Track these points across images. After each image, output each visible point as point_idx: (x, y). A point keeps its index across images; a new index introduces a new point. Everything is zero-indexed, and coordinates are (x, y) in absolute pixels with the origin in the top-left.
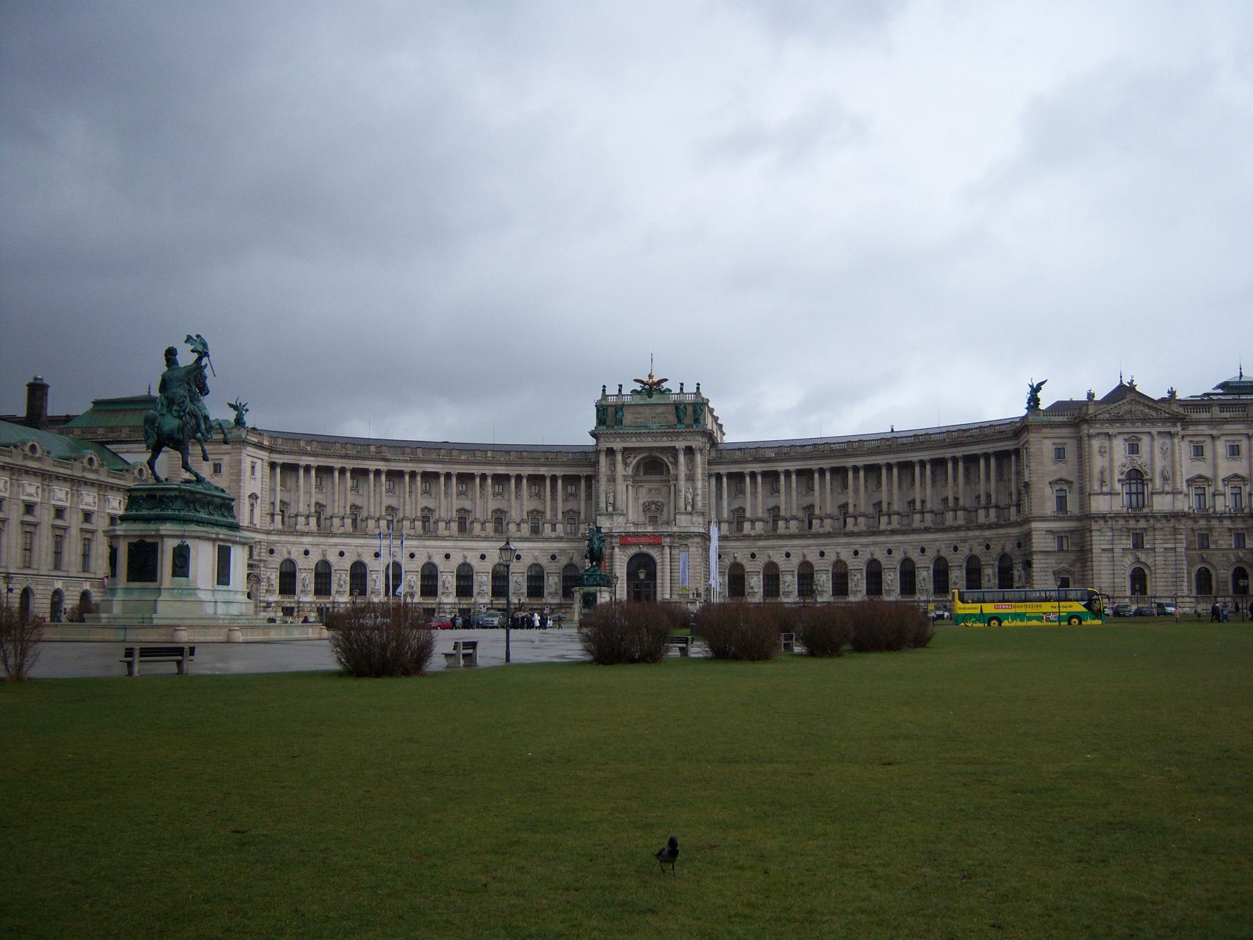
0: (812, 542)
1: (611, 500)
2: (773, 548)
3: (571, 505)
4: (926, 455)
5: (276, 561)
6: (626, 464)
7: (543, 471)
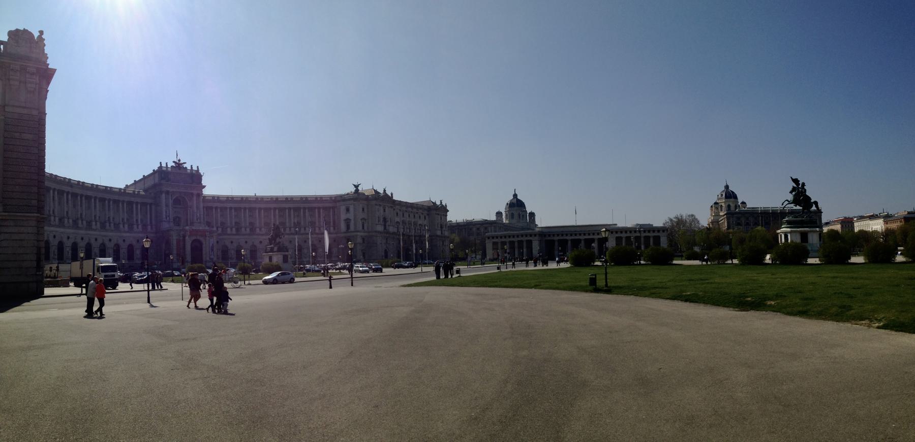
4: (291, 205)
7: (132, 199)
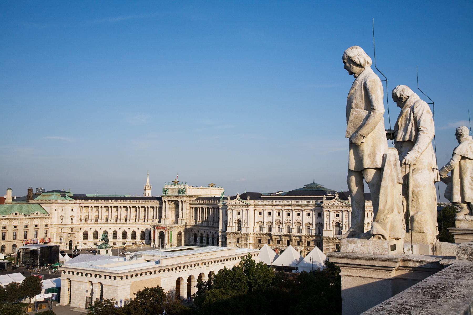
0: (208, 228)
5: (82, 231)
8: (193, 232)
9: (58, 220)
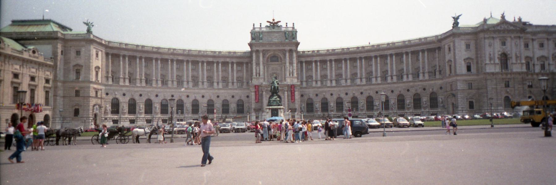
0: (342, 89)
1: (258, 72)
2: (325, 92)
3: (240, 74)
6: (263, 57)
7: (228, 60)
8: (306, 98)
9: (66, 71)
